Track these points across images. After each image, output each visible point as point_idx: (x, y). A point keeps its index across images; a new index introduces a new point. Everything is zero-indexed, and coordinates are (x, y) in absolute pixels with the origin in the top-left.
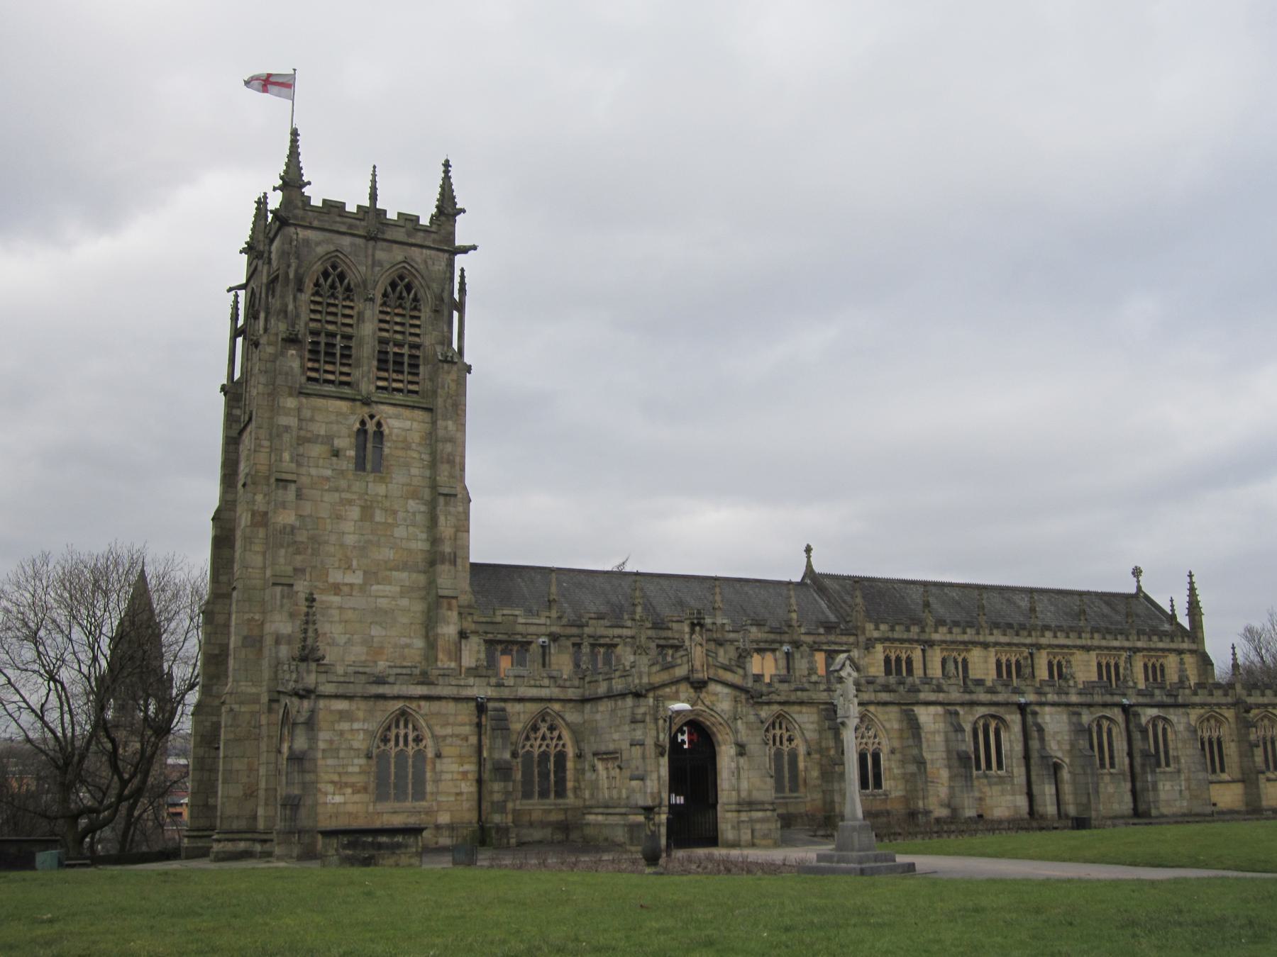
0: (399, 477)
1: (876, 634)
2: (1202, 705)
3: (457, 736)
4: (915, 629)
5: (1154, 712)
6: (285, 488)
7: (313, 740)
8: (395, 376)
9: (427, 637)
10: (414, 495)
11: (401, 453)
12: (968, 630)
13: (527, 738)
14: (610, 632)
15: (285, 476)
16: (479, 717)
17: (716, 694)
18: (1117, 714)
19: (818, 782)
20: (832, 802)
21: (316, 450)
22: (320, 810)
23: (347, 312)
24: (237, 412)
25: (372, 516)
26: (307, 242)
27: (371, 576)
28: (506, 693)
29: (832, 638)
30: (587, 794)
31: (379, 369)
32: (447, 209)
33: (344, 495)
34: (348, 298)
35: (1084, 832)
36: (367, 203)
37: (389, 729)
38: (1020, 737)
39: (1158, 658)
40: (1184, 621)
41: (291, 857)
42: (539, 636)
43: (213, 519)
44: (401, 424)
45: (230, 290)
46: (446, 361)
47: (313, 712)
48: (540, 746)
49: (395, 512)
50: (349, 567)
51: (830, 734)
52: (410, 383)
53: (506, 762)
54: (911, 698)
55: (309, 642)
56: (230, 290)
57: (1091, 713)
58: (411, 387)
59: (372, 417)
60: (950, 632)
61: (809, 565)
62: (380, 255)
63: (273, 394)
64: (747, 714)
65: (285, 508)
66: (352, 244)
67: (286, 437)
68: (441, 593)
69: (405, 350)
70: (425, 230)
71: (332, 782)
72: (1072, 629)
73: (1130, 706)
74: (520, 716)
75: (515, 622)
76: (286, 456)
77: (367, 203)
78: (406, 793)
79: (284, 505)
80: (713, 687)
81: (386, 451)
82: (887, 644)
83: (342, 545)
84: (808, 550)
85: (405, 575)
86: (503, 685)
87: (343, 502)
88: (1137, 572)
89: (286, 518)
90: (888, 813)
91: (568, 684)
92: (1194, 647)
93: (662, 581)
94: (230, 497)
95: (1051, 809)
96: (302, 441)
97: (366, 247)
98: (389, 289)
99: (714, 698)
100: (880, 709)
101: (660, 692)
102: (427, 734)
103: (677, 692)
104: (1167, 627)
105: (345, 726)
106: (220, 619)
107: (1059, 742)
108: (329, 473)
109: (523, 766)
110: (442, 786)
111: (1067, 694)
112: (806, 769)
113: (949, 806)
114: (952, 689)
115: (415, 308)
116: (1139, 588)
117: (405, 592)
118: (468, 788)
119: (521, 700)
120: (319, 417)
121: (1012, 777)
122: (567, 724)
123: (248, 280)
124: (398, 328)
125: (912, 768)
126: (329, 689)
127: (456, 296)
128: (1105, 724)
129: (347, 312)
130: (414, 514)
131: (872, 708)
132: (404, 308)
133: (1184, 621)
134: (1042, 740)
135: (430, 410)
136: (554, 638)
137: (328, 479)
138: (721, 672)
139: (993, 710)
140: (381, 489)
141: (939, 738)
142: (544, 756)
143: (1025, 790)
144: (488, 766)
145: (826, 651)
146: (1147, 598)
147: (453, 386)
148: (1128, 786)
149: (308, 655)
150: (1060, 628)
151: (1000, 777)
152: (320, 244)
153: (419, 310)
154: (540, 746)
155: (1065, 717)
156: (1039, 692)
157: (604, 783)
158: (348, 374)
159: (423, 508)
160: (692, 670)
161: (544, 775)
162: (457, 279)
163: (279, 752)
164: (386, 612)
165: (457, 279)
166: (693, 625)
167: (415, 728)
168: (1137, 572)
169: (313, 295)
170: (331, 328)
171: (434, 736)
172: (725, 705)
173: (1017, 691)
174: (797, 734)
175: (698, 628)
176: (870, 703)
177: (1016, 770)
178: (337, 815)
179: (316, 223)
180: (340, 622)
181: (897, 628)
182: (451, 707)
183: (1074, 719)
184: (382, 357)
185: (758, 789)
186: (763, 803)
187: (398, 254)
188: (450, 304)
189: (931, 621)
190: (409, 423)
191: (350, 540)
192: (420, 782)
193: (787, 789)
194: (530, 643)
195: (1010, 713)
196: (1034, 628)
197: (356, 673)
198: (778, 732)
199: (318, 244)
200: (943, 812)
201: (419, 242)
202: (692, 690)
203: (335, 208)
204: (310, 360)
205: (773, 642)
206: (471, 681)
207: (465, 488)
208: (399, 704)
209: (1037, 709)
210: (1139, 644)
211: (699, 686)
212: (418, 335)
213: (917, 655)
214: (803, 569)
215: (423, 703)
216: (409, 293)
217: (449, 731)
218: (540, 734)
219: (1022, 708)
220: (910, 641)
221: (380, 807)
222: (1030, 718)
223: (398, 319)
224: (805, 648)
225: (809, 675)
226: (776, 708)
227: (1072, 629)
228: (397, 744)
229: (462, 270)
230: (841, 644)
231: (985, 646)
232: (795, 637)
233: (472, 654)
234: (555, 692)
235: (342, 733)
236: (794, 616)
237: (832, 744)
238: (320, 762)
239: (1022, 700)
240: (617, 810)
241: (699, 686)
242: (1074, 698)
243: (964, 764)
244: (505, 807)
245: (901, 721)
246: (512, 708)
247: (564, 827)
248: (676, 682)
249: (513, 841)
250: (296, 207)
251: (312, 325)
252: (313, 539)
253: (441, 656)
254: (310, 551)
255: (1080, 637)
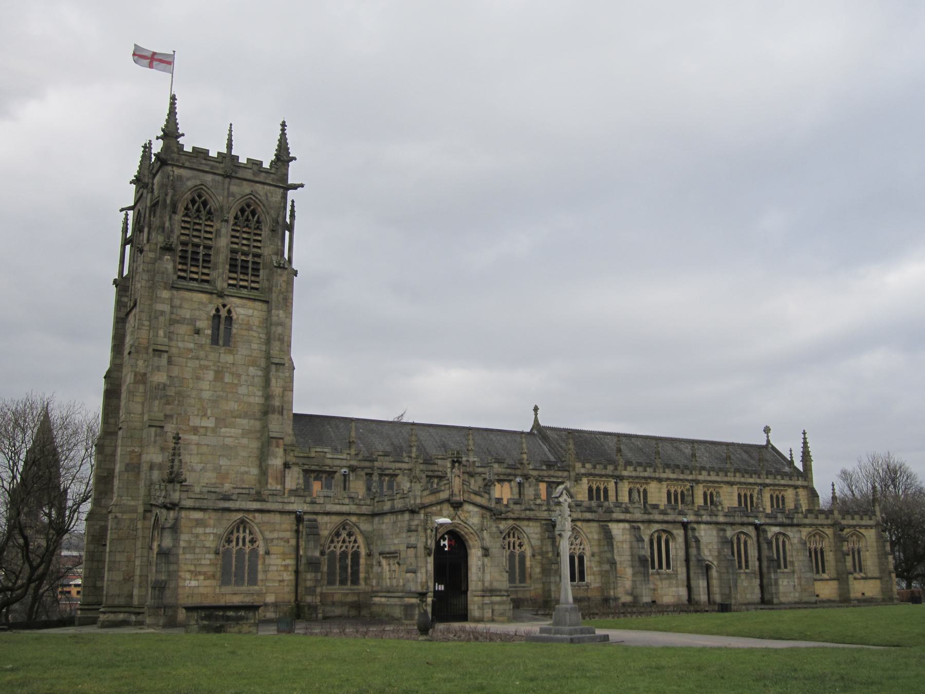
0: (243, 350)
1: (583, 471)
2: (811, 525)
3: (281, 539)
4: (610, 468)
5: (776, 529)
6: (160, 356)
7: (176, 540)
8: (242, 277)
9: (260, 466)
10: (254, 363)
11: (244, 333)
12: (648, 469)
13: (332, 541)
14: (393, 466)
15: (159, 348)
16: (298, 525)
17: (469, 512)
18: (751, 531)
19: (540, 576)
20: (550, 590)
21: (183, 329)
22: (180, 591)
23: (208, 229)
24: (125, 299)
25: (222, 379)
26: (180, 178)
27: (221, 421)
28: (317, 508)
29: (552, 473)
30: (374, 582)
31: (230, 271)
32: (283, 157)
33: (202, 362)
34: (209, 219)
35: (727, 614)
36: (225, 151)
37: (232, 533)
38: (683, 545)
39: (780, 491)
40: (799, 465)
41: (158, 626)
42: (342, 467)
43: (105, 377)
44: (245, 312)
45: (122, 210)
46: (279, 267)
47: (177, 520)
48: (341, 547)
49: (239, 376)
50: (205, 415)
51: (549, 542)
52: (252, 282)
53: (317, 558)
54: (606, 517)
55: (175, 469)
56: (122, 210)
57: (733, 530)
58: (253, 285)
59: (224, 306)
60: (635, 470)
61: (536, 420)
62: (234, 189)
63: (152, 287)
64: (491, 526)
65: (159, 371)
66: (213, 180)
67: (161, 319)
68: (272, 435)
69: (250, 258)
70: (267, 172)
71: (189, 571)
72: (721, 470)
73: (761, 525)
74: (327, 525)
75: (325, 457)
76: (161, 333)
77: (225, 151)
78: (243, 580)
79: (158, 368)
80: (467, 507)
81: (234, 331)
82: (591, 478)
83: (200, 399)
84: (536, 409)
85: (245, 421)
86: (315, 503)
87: (202, 368)
88: (767, 430)
89: (160, 378)
90: (589, 599)
91: (362, 502)
92: (805, 484)
93: (431, 430)
94: (118, 361)
95: (703, 598)
96: (172, 322)
97: (223, 183)
98: (239, 213)
99: (467, 515)
100: (585, 524)
101: (428, 510)
102: (260, 537)
103: (441, 510)
104: (787, 469)
105: (200, 530)
106: (108, 450)
107: (710, 550)
108: (192, 346)
109: (329, 561)
110: (270, 575)
111: (716, 516)
112: (531, 566)
113: (631, 594)
114: (636, 510)
115: (258, 228)
116: (768, 441)
117: (246, 433)
118: (289, 576)
119: (328, 514)
120: (186, 305)
121: (676, 575)
122: (361, 532)
123: (136, 204)
124: (245, 242)
125: (606, 567)
126: (188, 503)
127: (288, 220)
128: (743, 537)
129: (208, 229)
130: (253, 377)
131: (579, 524)
132: (250, 228)
133: (799, 465)
134: (698, 548)
135: (267, 302)
136: (353, 469)
137: (191, 350)
138: (473, 496)
139: (664, 526)
140: (229, 358)
141: (626, 546)
142: (344, 555)
143: (685, 583)
144: (304, 561)
145: (547, 482)
146: (773, 448)
147: (284, 285)
148: (758, 581)
149: (174, 478)
150: (712, 469)
151: (668, 574)
152: (190, 179)
153: (261, 230)
154: (341, 547)
155: (715, 533)
156: (697, 514)
157: (387, 574)
158: (208, 275)
159: (260, 373)
160: (452, 495)
161: (344, 568)
162: (289, 208)
163: (151, 548)
164: (231, 448)
165: (289, 208)
166: (453, 462)
167: (251, 533)
168: (767, 430)
169: (184, 216)
170: (196, 240)
171: (265, 539)
172: (475, 520)
173: (681, 513)
174: (525, 541)
175: (457, 465)
176: (579, 520)
177: (679, 570)
178: (192, 595)
179: (187, 164)
180: (198, 454)
181: (598, 466)
182: (277, 518)
183: (721, 534)
184: (234, 263)
185: (497, 581)
186: (501, 591)
187: (247, 188)
188: (283, 226)
189: (621, 462)
190: (251, 311)
191: (206, 395)
192: (253, 571)
193: (517, 581)
194: (335, 472)
195: (677, 529)
196: (694, 468)
197: (209, 492)
198: (512, 540)
199: (188, 179)
200: (628, 599)
201: (262, 180)
202: (451, 509)
203: (200, 153)
204: (180, 263)
205: (510, 475)
206: (293, 499)
207: (291, 359)
208: (240, 515)
209: (695, 526)
210: (768, 481)
211: (457, 506)
212: (259, 248)
213: (611, 486)
214: (532, 423)
215: (257, 515)
216: (253, 217)
217: (275, 535)
218: (341, 539)
219: (685, 525)
220: (607, 476)
221: (225, 589)
222: (690, 533)
223: (245, 236)
224: (532, 479)
225: (535, 499)
226: (511, 522)
227: (721, 470)
228: (237, 544)
229: (293, 201)
230: (557, 477)
231: (660, 480)
232: (525, 472)
233: (293, 479)
234: (353, 508)
235: (197, 536)
236: (525, 456)
237: (550, 549)
238: (181, 557)
239: (685, 520)
240: (396, 594)
241: (457, 506)
242: (721, 519)
243: (643, 564)
244: (315, 591)
245: (599, 533)
246: (321, 519)
247: (357, 606)
248: (440, 503)
249: (320, 616)
250: (173, 152)
251: (183, 238)
252: (179, 394)
253: (270, 480)
254: (176, 402)
255: (726, 476)
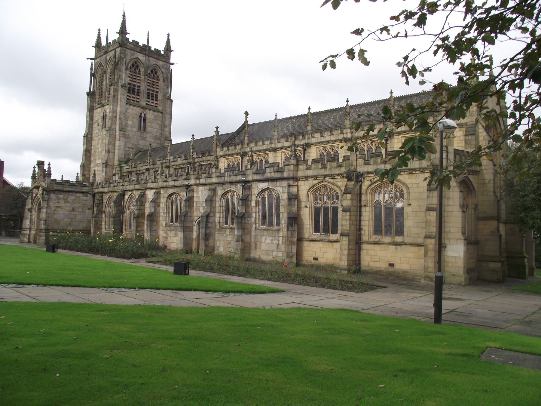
5: (264, 185)
57: (224, 189)
242: (214, 180)
